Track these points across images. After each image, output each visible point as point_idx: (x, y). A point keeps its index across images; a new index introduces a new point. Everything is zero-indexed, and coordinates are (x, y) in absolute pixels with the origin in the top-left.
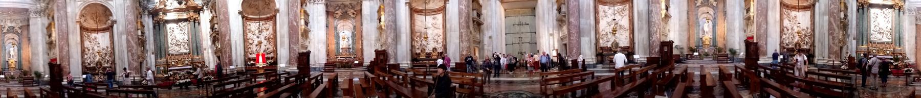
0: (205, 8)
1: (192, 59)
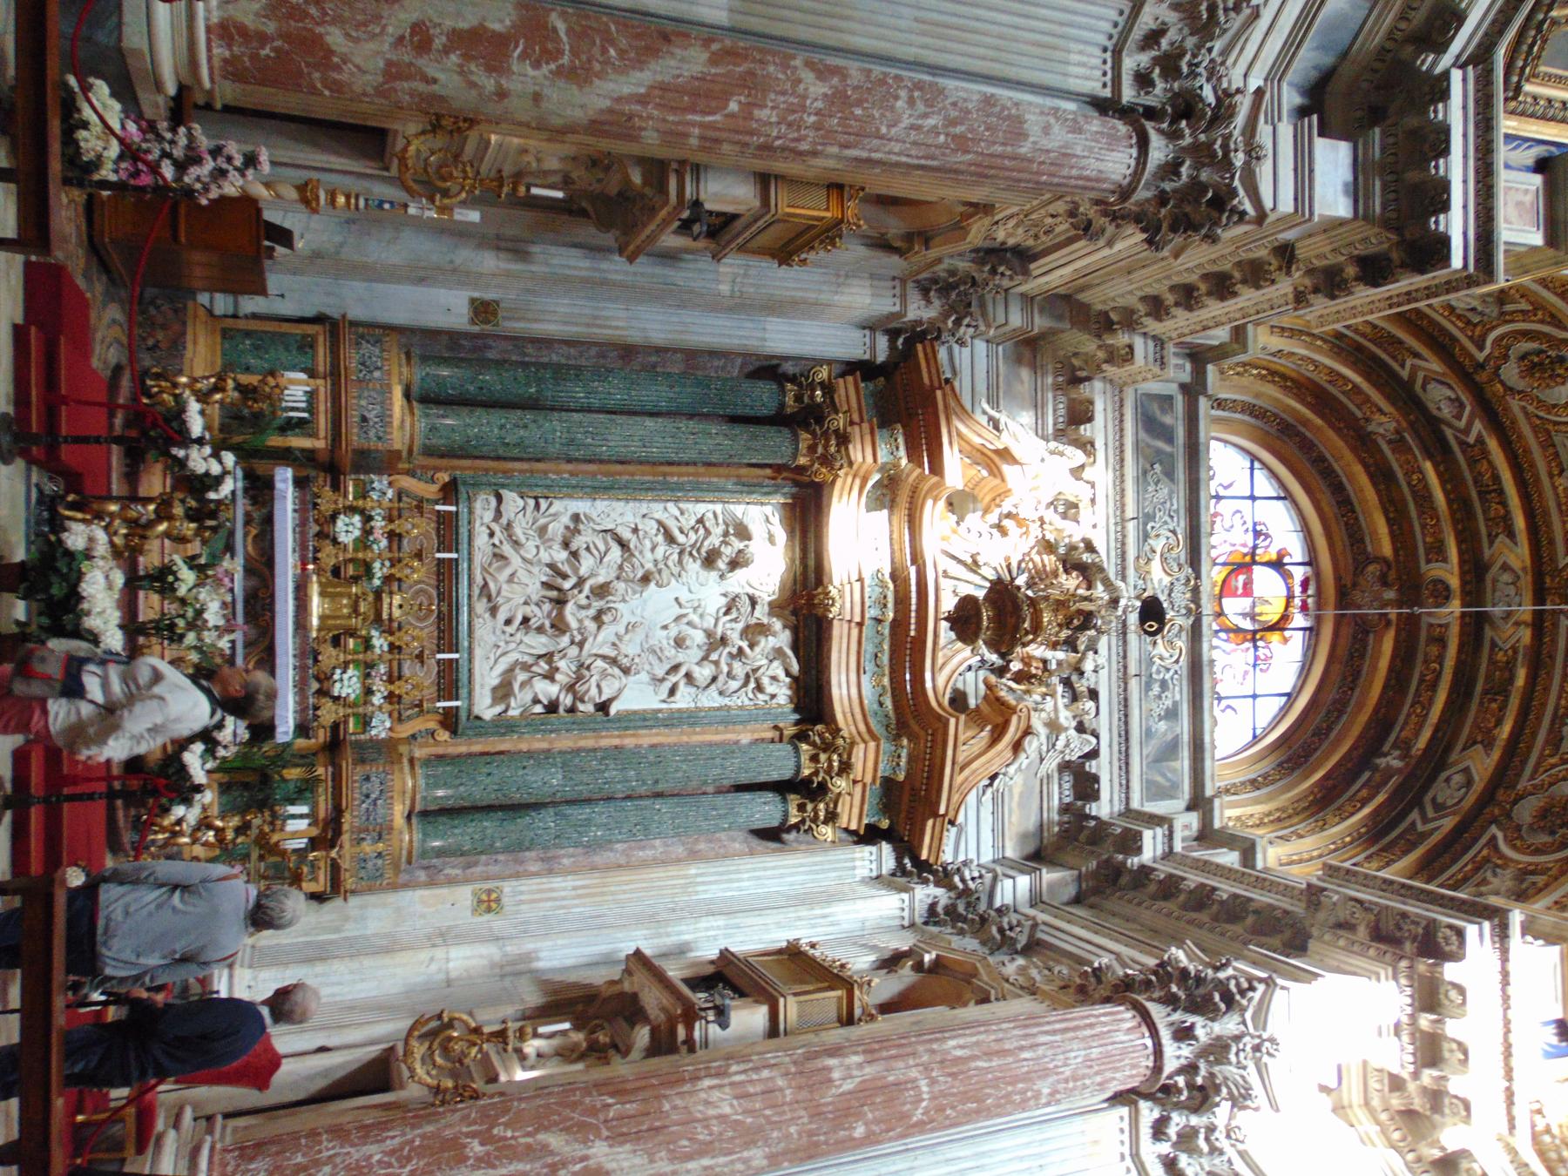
0: (926, 893)
1: (387, 750)
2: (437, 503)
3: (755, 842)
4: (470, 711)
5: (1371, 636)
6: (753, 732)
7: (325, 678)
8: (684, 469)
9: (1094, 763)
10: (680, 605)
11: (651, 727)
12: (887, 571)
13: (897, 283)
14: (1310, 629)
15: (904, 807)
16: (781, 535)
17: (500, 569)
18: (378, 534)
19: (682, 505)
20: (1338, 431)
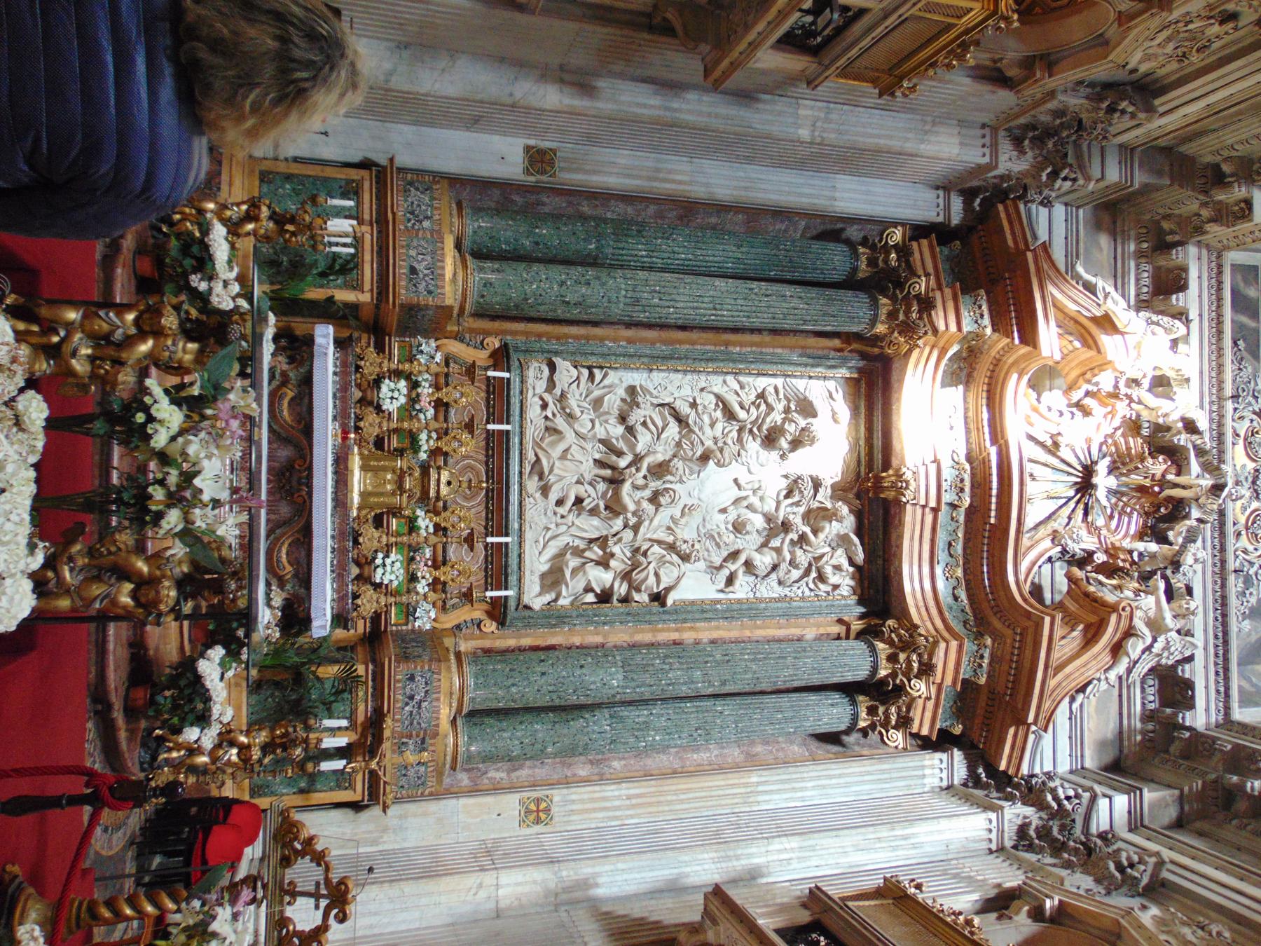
0: (1016, 813)
1: (431, 642)
2: (487, 369)
3: (814, 745)
4: (519, 599)
6: (818, 626)
7: (365, 563)
8: (748, 337)
9: (1187, 667)
10: (739, 487)
11: (710, 619)
12: (962, 452)
13: (987, 131)
15: (980, 712)
16: (844, 412)
17: (553, 444)
18: (425, 402)
19: (741, 378)
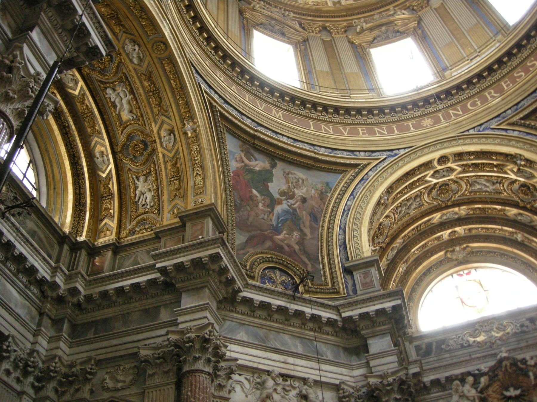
5: (474, 250)
14: (475, 270)
20: (407, 282)
